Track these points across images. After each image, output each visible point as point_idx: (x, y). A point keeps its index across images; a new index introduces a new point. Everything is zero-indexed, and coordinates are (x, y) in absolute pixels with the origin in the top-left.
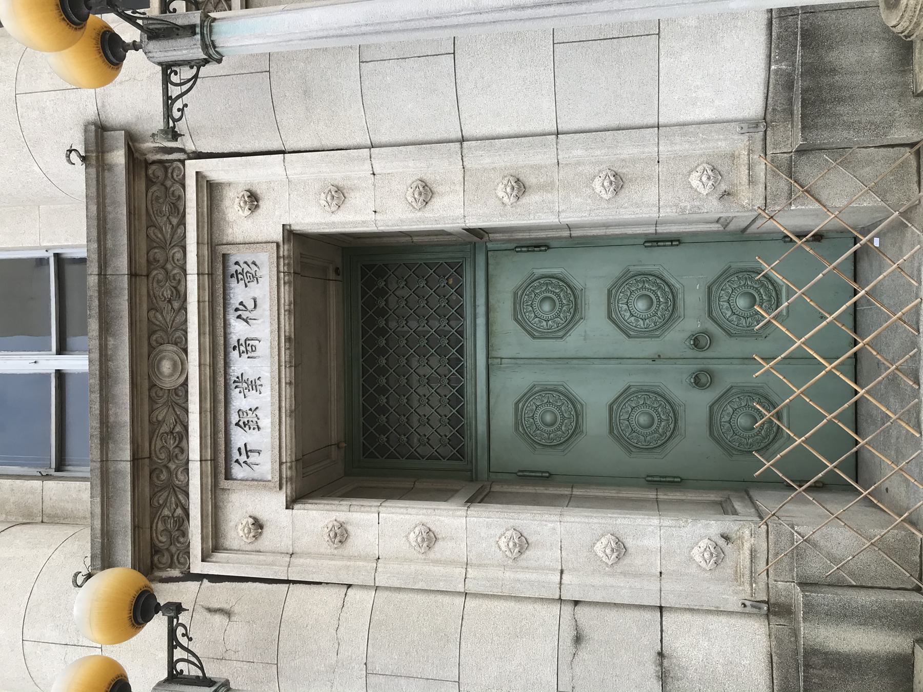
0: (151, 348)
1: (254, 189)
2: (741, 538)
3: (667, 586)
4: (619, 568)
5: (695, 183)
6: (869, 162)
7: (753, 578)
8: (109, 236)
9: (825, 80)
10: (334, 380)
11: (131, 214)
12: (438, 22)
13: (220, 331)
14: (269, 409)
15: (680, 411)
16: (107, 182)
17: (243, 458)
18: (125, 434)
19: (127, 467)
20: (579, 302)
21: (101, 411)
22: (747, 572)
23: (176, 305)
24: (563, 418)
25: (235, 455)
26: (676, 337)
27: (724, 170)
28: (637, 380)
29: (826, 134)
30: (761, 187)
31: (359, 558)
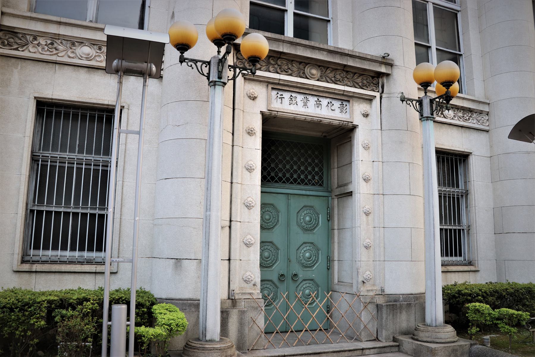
1: (369, 116)
2: (255, 290)
3: (238, 262)
4: (242, 244)
5: (368, 273)
6: (373, 326)
7: (243, 294)
8: (359, 60)
9: (398, 311)
10: (285, 130)
11: (365, 70)
13: (324, 95)
14: (297, 110)
16: (376, 64)
17: (279, 96)
19: (281, 50)
20: (309, 232)
22: (244, 292)
23: (333, 79)
25: (280, 93)
26: (296, 268)
27: (370, 282)
30: (366, 294)
31: (243, 140)
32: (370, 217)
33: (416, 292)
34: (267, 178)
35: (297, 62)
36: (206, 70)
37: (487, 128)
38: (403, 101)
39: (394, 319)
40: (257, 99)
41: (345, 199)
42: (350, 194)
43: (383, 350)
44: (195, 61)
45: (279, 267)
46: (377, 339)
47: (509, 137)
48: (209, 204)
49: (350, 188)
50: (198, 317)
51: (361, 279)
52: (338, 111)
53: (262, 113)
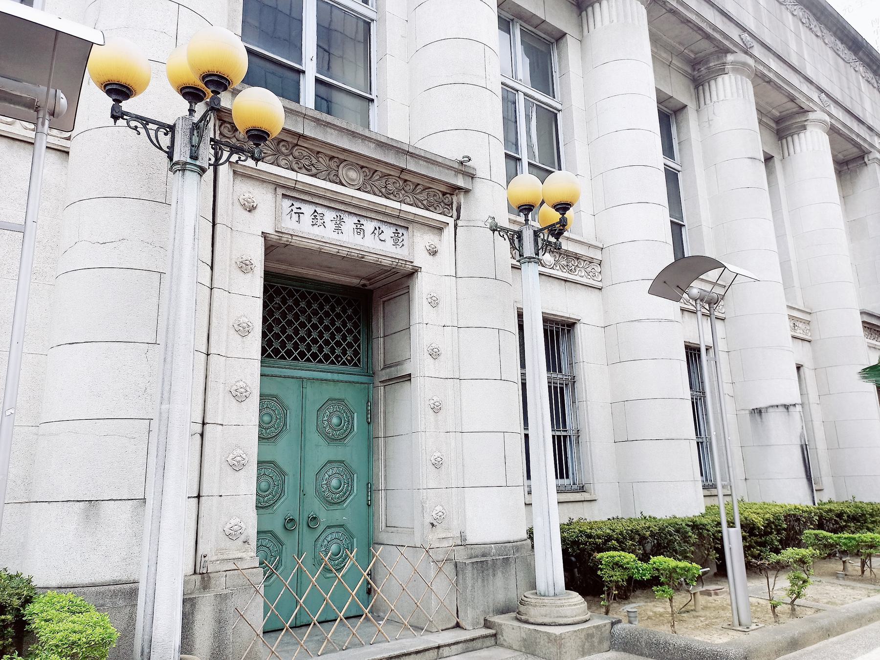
0: (362, 167)
9: (491, 571)
10: (300, 270)
11: (433, 179)
12: (537, 377)
13: (369, 214)
15: (270, 511)
17: (295, 210)
18: (320, 137)
19: (301, 132)
21: (334, 125)
22: (225, 557)
23: (383, 190)
24: (266, 429)
26: (316, 507)
28: (290, 481)
29: (470, 575)
32: (441, 415)
33: (516, 538)
34: (271, 350)
35: (326, 155)
36: (165, 141)
37: (599, 285)
38: (494, 231)
39: (484, 586)
40: (257, 211)
41: (397, 386)
42: (408, 377)
43: (471, 644)
44: (145, 121)
45: (285, 507)
46: (458, 626)
47: (651, 291)
48: (167, 388)
49: (407, 369)
50: (132, 618)
51: (428, 520)
52: (390, 242)
53: (264, 235)
